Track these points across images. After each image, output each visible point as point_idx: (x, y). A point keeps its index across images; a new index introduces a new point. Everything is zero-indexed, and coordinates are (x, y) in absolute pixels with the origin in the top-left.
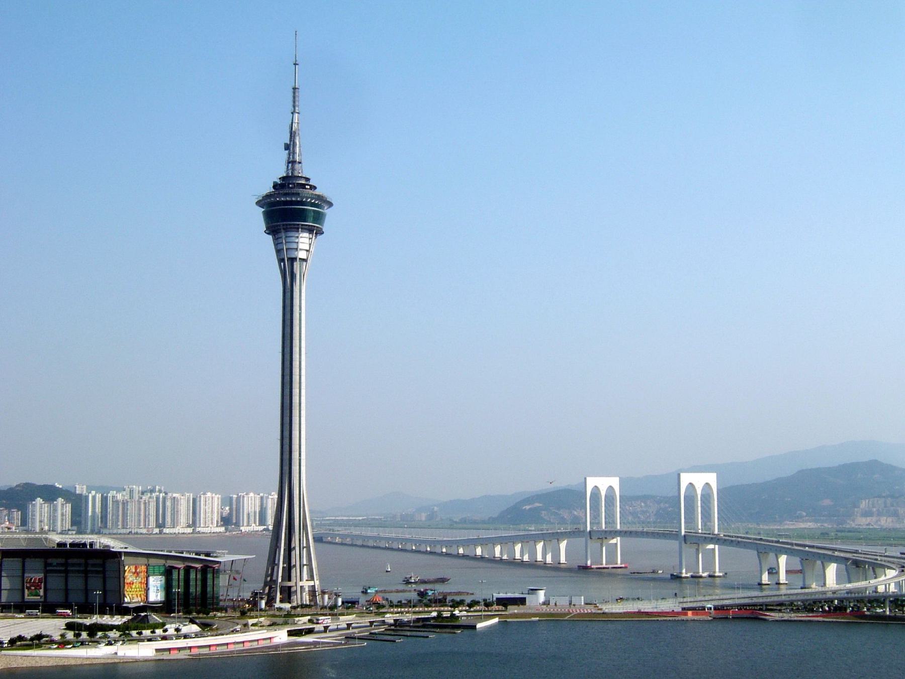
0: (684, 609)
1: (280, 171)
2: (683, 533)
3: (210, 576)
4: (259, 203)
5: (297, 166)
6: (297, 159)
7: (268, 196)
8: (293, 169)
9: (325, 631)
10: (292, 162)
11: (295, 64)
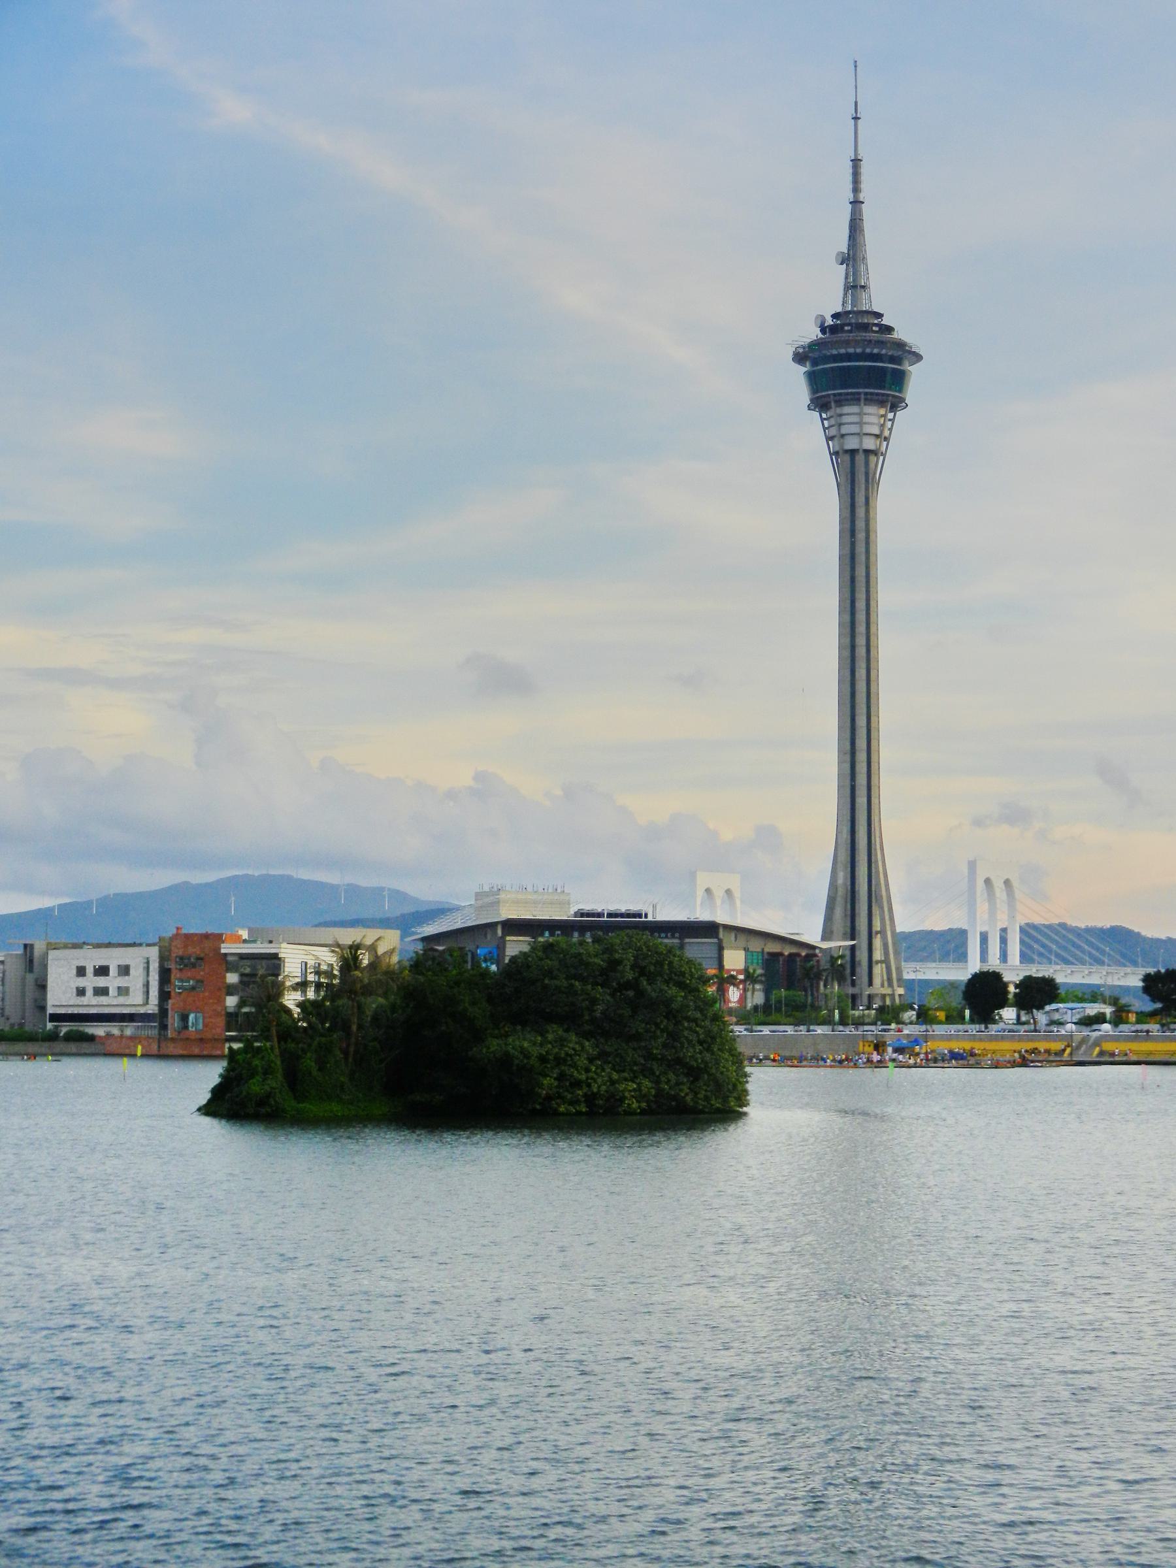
1: (832, 302)
4: (799, 358)
5: (864, 295)
7: (814, 345)
10: (854, 287)
11: (856, 118)
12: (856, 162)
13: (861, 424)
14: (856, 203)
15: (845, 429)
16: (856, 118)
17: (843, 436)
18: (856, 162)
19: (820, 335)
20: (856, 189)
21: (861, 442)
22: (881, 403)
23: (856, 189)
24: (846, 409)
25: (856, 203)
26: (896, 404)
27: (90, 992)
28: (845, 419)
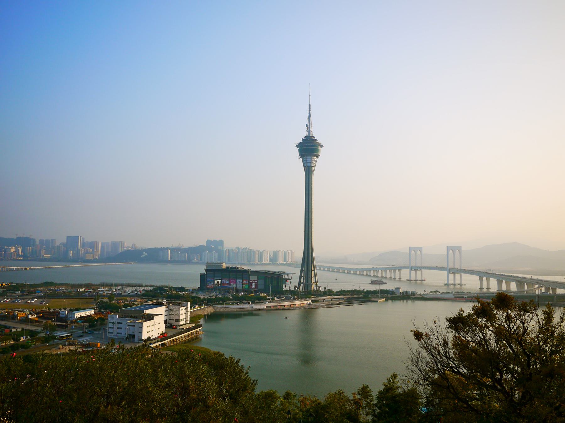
1: (305, 134)
4: (297, 146)
8: (309, 133)
10: (309, 131)
11: (310, 95)
12: (310, 104)
13: (311, 160)
14: (310, 113)
15: (308, 161)
16: (310, 95)
17: (307, 163)
18: (310, 104)
19: (302, 141)
20: (310, 110)
21: (311, 165)
23: (310, 110)
24: (308, 157)
25: (310, 113)
26: (318, 156)
27: (124, 316)
28: (308, 159)
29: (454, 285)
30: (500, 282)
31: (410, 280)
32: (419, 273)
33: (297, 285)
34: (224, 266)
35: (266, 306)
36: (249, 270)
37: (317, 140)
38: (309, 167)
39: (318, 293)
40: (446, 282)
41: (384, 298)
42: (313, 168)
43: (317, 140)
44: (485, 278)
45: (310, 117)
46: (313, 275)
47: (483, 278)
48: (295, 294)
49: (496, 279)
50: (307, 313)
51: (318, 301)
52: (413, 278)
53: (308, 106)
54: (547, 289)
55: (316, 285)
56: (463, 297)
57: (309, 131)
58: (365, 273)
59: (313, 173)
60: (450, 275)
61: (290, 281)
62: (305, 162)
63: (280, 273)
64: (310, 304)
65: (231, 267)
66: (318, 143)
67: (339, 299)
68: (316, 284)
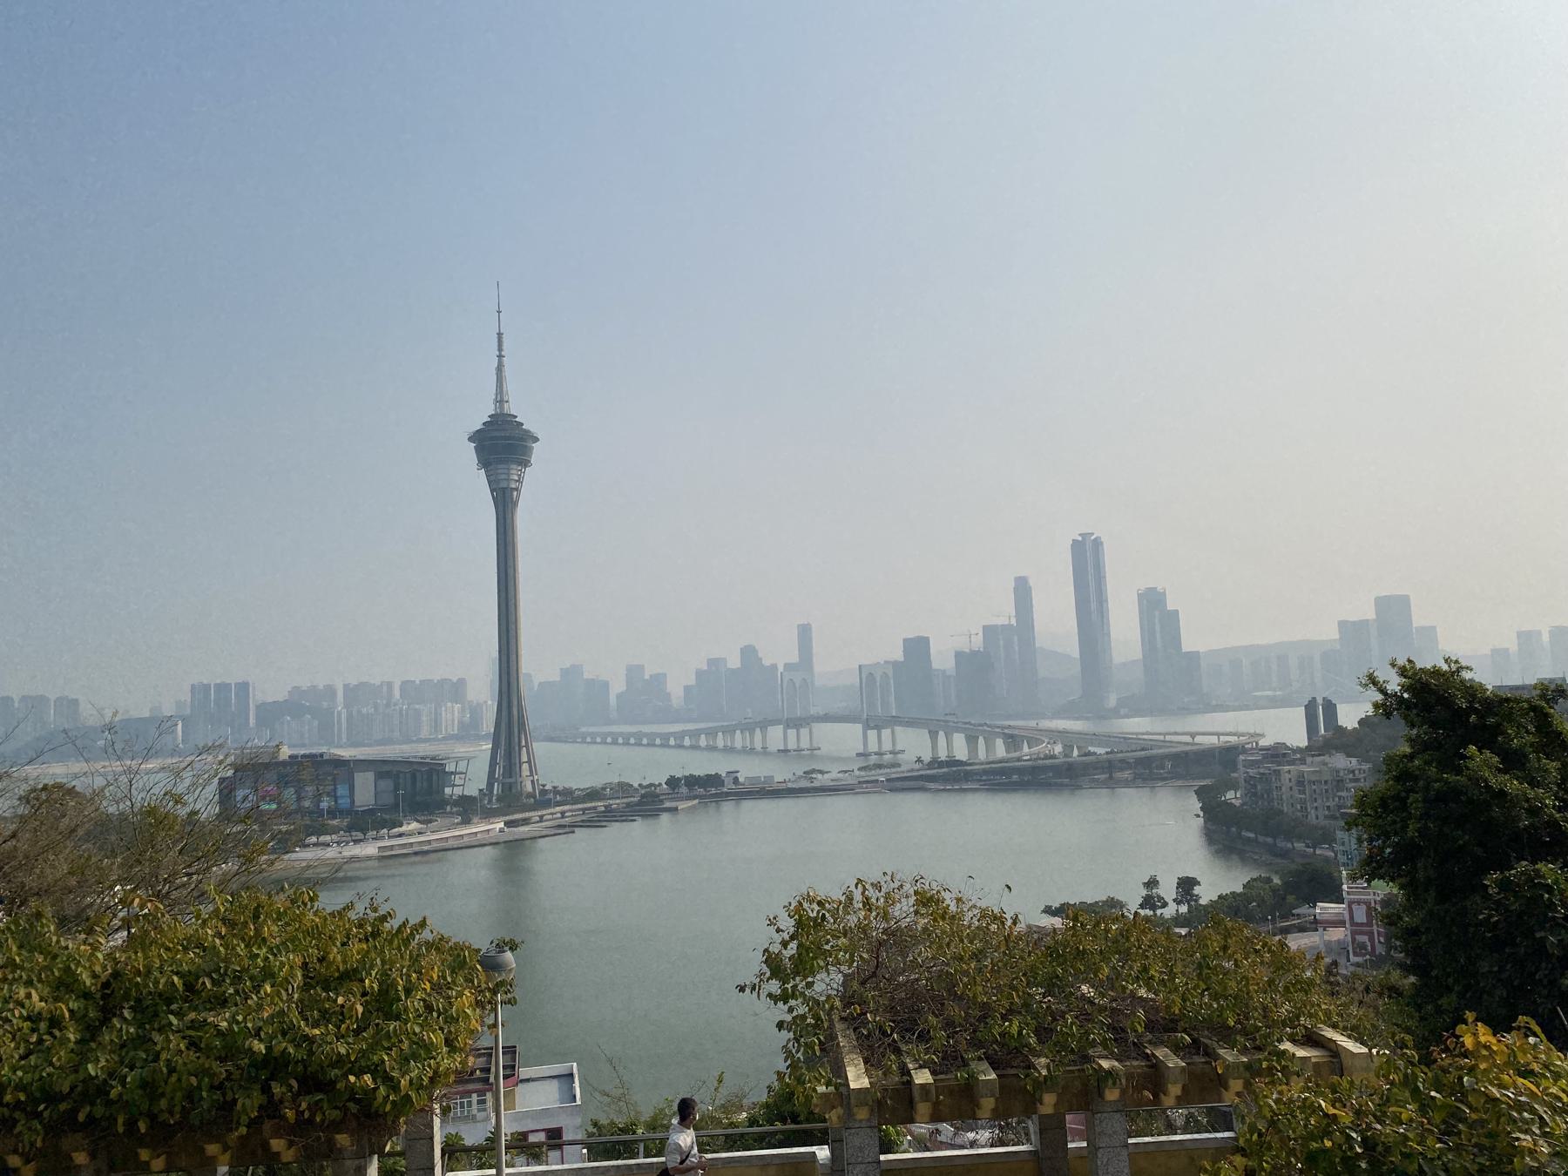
0: (860, 782)
2: (865, 716)
3: (435, 777)
4: (470, 439)
5: (506, 405)
6: (505, 399)
8: (502, 407)
9: (541, 821)
10: (500, 400)
11: (499, 312)
12: (500, 335)
13: (508, 474)
14: (500, 356)
16: (499, 312)
18: (500, 335)
20: (500, 349)
22: (520, 464)
23: (500, 349)
25: (500, 356)
28: (500, 471)
29: (880, 754)
30: (971, 740)
31: (786, 751)
32: (804, 732)
33: (483, 786)
34: (285, 753)
35: (379, 848)
36: (353, 758)
37: (522, 424)
38: (504, 490)
39: (544, 799)
40: (861, 751)
41: (694, 799)
42: (515, 493)
43: (522, 424)
44: (941, 733)
45: (500, 369)
46: (524, 758)
47: (937, 732)
48: (468, 808)
49: (963, 735)
50: (513, 852)
51: (526, 822)
52: (792, 745)
53: (497, 340)
54: (1068, 748)
55: (533, 782)
56: (878, 780)
57: (500, 400)
58: (599, 740)
59: (515, 504)
60: (789, 731)
61: (463, 776)
62: (492, 478)
63: (439, 760)
64: (501, 830)
65: (302, 753)
66: (527, 432)
67: (584, 810)
68: (531, 778)
